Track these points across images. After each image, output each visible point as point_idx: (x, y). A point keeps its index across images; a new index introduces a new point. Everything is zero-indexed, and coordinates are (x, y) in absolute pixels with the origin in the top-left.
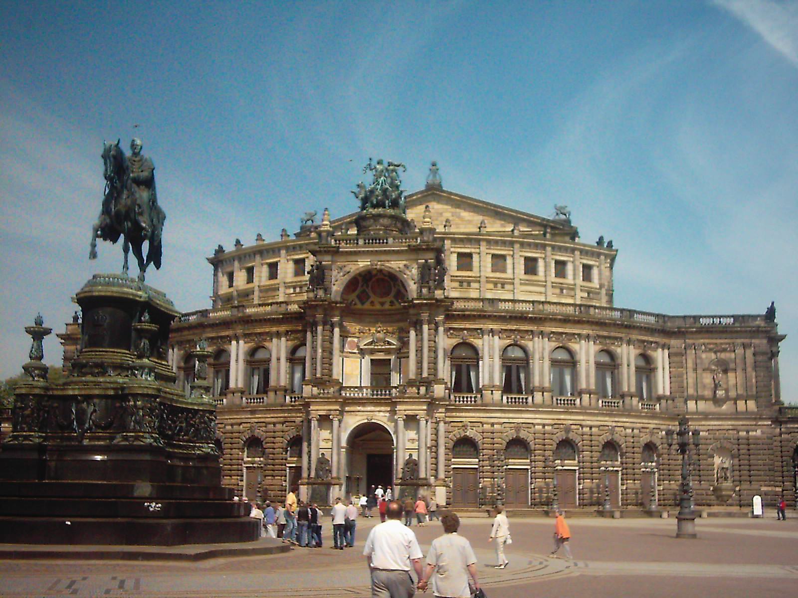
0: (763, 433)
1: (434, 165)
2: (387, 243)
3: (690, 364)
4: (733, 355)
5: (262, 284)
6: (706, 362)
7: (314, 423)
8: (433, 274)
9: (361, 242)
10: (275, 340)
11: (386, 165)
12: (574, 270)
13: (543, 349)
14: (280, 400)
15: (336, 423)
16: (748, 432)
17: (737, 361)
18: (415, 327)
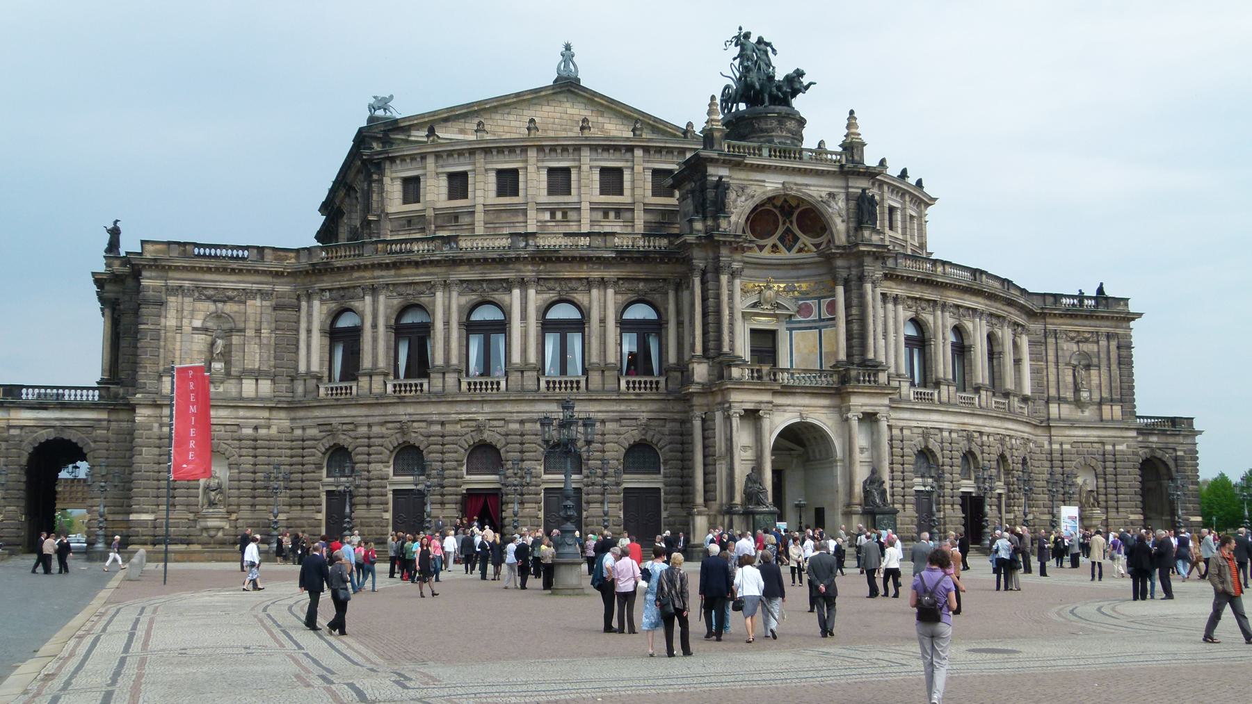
0: (1128, 446)
1: (568, 47)
2: (801, 158)
3: (1051, 358)
4: (1095, 348)
5: (489, 202)
6: (1068, 354)
7: (736, 421)
8: (864, 211)
9: (765, 152)
10: (595, 292)
11: (753, 40)
12: (904, 221)
13: (944, 326)
14: (611, 385)
15: (766, 423)
16: (1114, 446)
17: (1102, 355)
18: (845, 286)
